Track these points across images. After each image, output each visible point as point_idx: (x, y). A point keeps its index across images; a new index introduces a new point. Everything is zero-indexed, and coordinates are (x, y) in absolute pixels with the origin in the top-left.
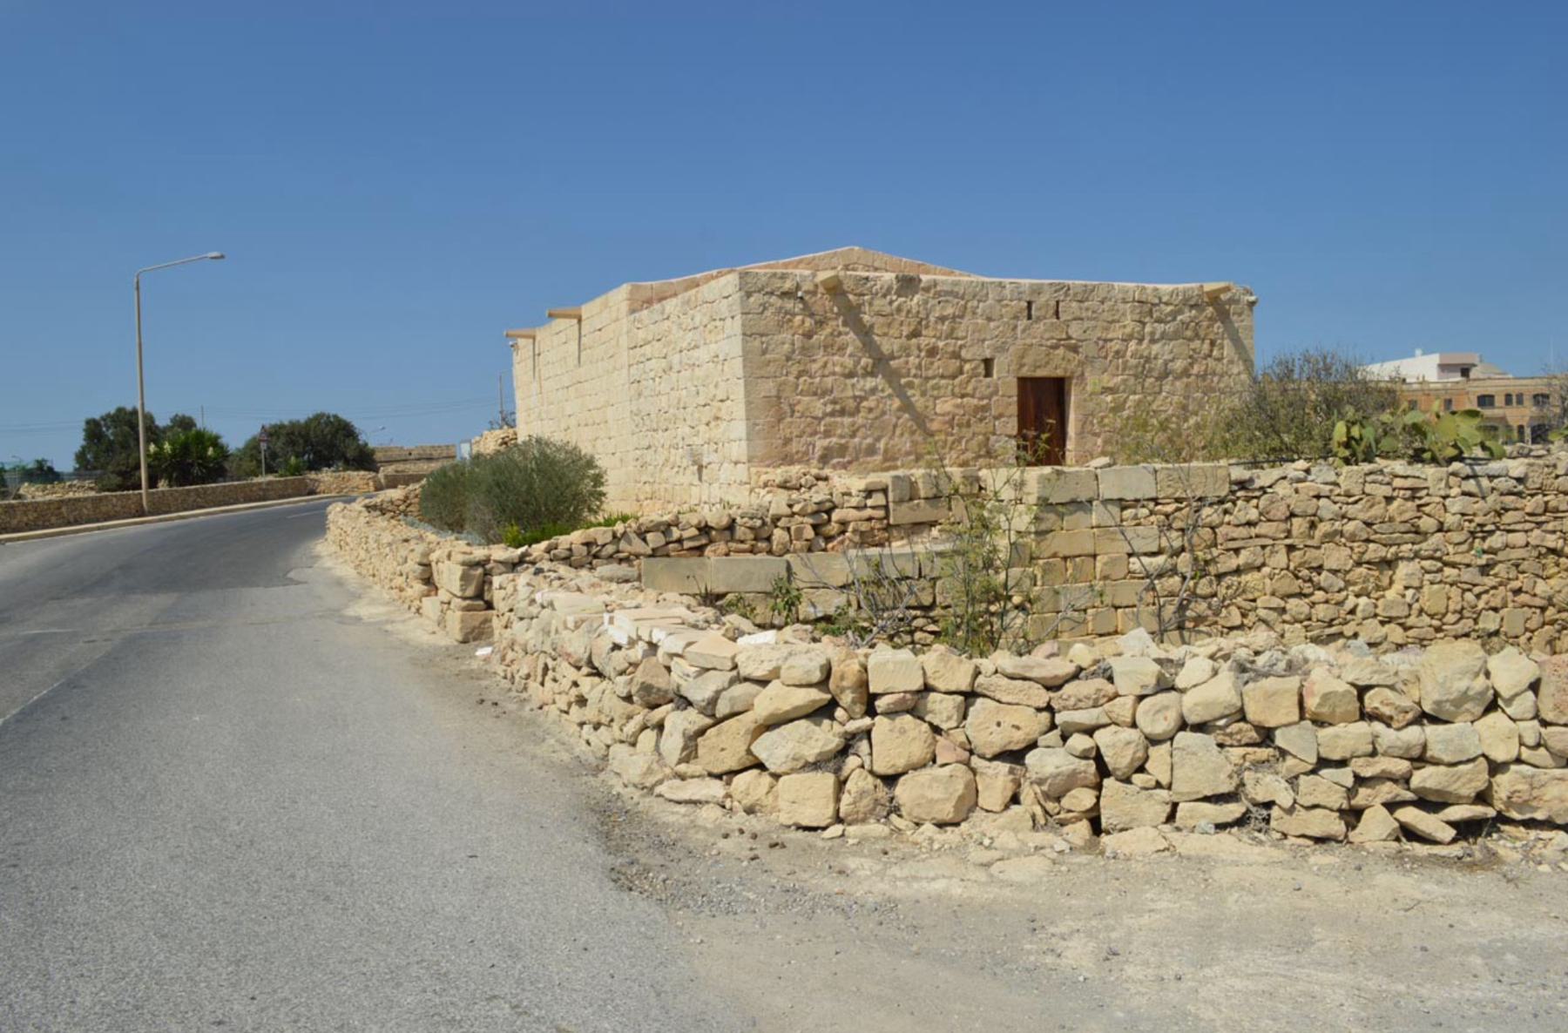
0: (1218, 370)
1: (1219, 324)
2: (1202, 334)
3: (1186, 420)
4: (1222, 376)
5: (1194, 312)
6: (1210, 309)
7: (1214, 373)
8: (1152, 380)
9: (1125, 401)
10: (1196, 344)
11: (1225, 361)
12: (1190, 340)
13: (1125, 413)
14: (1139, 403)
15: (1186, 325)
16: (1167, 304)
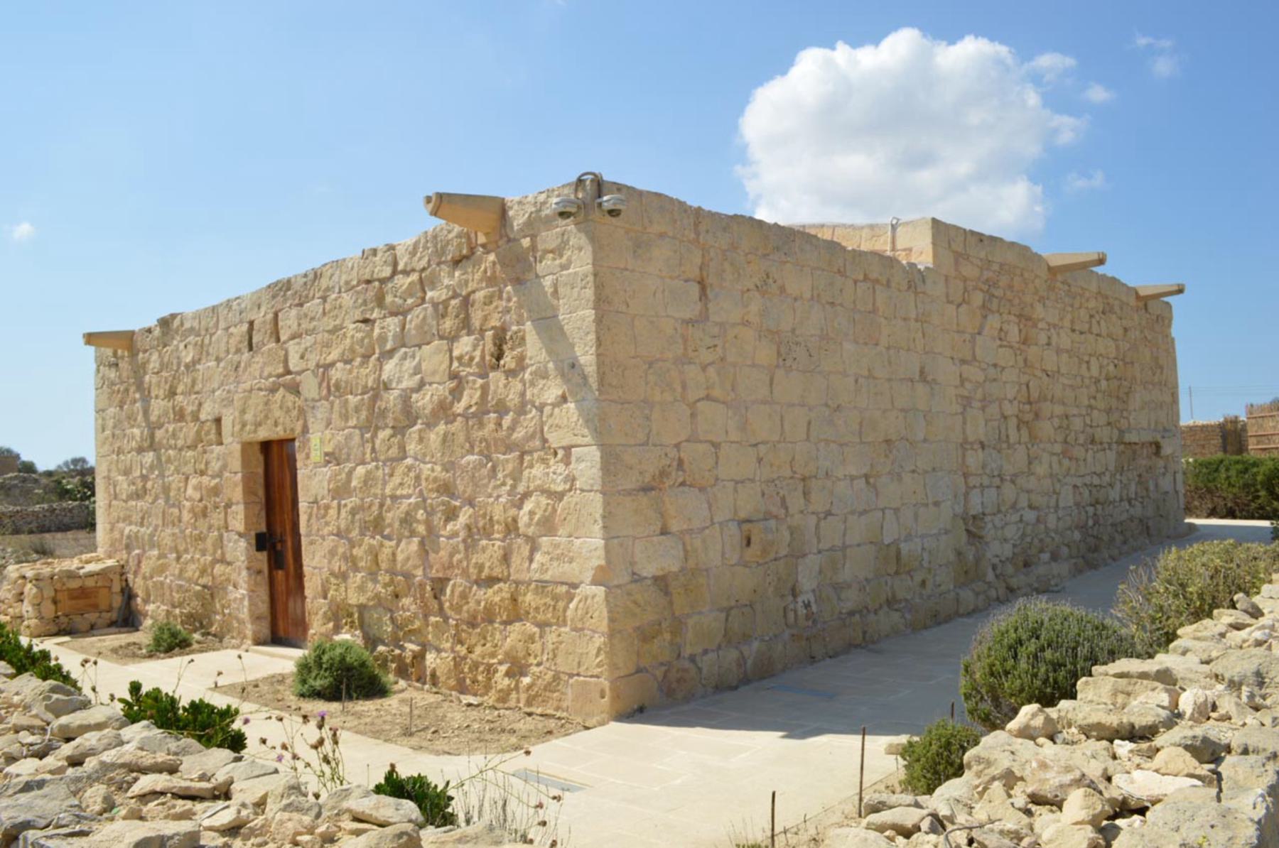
0: (513, 399)
1: (509, 288)
2: (476, 319)
3: (451, 515)
4: (521, 410)
5: (457, 274)
6: (492, 257)
7: (501, 409)
8: (388, 432)
9: (350, 473)
10: (464, 345)
11: (527, 376)
12: (452, 339)
13: (352, 501)
14: (368, 480)
15: (441, 310)
16: (406, 273)
